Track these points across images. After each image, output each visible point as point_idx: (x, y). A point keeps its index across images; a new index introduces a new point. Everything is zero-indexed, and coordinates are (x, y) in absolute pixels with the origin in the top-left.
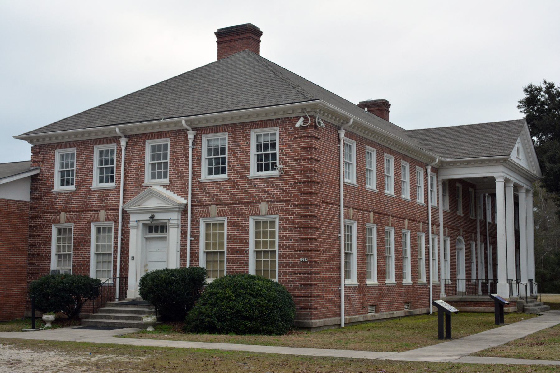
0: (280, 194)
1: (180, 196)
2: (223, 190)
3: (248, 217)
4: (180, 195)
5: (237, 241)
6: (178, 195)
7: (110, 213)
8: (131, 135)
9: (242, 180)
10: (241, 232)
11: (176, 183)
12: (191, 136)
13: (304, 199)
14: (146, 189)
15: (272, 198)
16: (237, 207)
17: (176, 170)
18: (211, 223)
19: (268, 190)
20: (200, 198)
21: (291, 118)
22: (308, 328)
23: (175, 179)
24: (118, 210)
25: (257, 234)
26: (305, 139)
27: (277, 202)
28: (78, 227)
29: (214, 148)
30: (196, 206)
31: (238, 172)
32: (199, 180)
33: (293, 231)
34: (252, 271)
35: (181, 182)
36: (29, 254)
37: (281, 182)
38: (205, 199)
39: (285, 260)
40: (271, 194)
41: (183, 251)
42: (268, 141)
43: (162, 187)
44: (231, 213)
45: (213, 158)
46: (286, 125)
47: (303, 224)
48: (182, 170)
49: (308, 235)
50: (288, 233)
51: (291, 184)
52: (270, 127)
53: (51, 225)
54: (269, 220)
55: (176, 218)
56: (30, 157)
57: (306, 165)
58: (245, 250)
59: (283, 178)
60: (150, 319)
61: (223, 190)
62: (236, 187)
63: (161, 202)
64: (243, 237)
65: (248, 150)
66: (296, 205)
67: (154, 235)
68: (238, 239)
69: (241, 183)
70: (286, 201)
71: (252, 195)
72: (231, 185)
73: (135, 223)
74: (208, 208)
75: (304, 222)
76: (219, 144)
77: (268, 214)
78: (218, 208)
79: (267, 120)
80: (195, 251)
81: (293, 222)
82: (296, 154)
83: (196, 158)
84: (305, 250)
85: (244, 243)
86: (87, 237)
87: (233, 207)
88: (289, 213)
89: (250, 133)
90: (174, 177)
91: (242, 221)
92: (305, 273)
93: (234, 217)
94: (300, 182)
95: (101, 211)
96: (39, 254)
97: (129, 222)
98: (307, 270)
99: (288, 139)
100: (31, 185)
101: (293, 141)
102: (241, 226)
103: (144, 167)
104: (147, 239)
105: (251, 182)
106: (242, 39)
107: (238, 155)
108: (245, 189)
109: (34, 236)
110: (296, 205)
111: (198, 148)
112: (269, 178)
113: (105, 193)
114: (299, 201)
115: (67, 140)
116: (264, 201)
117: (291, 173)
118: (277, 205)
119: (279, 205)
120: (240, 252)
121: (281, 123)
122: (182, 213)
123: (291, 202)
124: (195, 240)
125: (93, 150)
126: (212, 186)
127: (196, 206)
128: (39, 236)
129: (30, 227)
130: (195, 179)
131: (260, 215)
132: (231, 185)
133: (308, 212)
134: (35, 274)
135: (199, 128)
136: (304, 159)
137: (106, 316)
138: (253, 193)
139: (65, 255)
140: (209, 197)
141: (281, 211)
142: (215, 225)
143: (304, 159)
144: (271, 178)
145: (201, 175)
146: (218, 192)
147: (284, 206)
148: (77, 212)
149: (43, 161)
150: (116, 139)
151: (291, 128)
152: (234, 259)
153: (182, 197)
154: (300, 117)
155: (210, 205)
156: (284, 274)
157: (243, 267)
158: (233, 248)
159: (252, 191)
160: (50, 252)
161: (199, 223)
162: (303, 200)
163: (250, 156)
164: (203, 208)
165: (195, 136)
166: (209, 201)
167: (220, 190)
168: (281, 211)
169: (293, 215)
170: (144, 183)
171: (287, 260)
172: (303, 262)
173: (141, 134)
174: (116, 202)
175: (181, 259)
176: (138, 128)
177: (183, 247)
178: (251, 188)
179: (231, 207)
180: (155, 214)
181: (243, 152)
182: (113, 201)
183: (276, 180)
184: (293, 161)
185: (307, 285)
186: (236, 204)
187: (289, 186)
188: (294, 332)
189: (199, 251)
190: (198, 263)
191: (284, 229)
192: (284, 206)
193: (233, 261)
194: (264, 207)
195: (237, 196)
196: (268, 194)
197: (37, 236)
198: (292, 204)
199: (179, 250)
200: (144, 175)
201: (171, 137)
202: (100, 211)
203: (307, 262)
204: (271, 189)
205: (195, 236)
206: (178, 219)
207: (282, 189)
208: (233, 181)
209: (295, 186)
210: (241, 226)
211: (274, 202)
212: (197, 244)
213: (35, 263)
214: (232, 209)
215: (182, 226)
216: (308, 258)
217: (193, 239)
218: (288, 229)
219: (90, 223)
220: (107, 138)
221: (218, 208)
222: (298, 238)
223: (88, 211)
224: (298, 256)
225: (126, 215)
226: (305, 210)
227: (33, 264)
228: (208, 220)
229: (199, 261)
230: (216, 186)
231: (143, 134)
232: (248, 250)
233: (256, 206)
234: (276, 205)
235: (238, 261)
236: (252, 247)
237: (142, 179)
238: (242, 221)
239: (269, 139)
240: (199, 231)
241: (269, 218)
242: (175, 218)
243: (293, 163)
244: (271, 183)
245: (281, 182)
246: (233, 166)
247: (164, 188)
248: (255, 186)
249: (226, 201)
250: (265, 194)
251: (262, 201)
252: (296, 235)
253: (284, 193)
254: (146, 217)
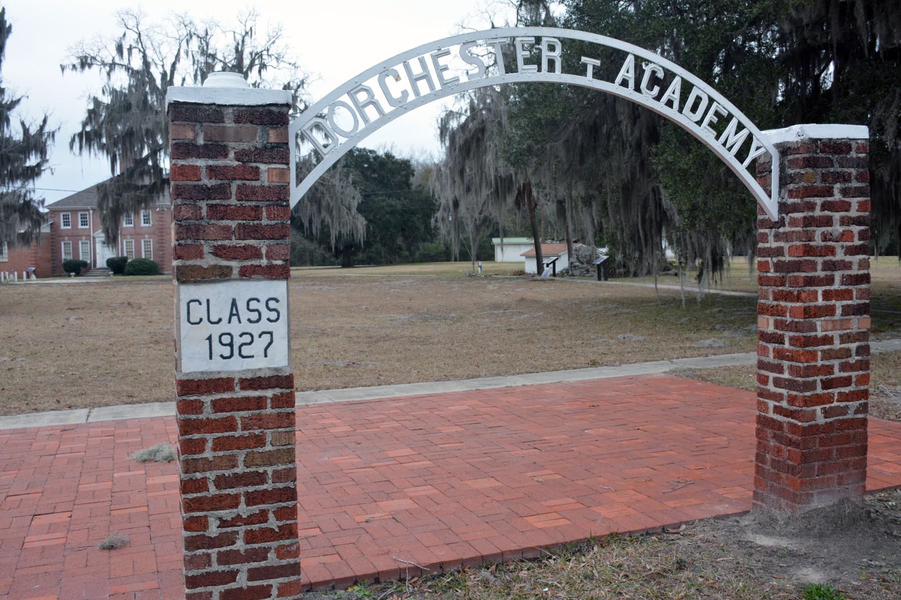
34: (143, 257)
38: (126, 233)
57: (160, 223)
60: (112, 273)
150: (88, 210)
162: (160, 234)
194: (147, 236)
225: (94, 238)
252: (158, 245)
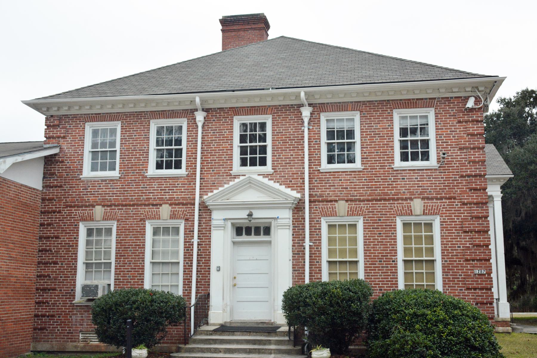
0: (440, 189)
1: (290, 189)
2: (356, 182)
3: (395, 217)
4: (289, 187)
5: (380, 248)
6: (286, 187)
7: (179, 209)
8: (211, 109)
9: (384, 171)
10: (385, 236)
11: (283, 171)
12: (306, 112)
13: (476, 196)
14: (235, 178)
15: (430, 194)
16: (378, 204)
17: (283, 156)
18: (337, 223)
19: (422, 184)
20: (321, 191)
21: (452, 98)
23: (281, 166)
24: (194, 204)
25: (407, 239)
26: (472, 123)
27: (437, 199)
28: (123, 227)
29: (347, 131)
30: (315, 201)
31: (377, 161)
32: (319, 168)
33: (461, 236)
34: (401, 286)
35: (291, 171)
36: (39, 263)
37: (441, 175)
38: (329, 193)
39: (452, 272)
40: (428, 189)
41: (296, 259)
42: (417, 125)
43: (261, 177)
44: (368, 212)
45: (335, 143)
46: (445, 106)
47: (477, 227)
48: (292, 155)
49: (485, 241)
50: (454, 239)
51: (455, 178)
52: (421, 107)
53: (79, 223)
54: (423, 222)
55: (288, 216)
56: (44, 130)
58: (392, 259)
59: (443, 170)
61: (356, 182)
62: (374, 179)
63: (262, 195)
64: (389, 242)
65: (391, 134)
66: (464, 204)
67: (244, 238)
68: (381, 245)
69: (382, 174)
70: (450, 198)
71: (400, 190)
72: (367, 177)
73: (222, 222)
74: (335, 205)
75: (478, 224)
76: (346, 126)
77: (424, 214)
78: (349, 205)
79: (417, 99)
80: (316, 259)
81: (461, 225)
82: (461, 141)
83: (313, 142)
84: (480, 260)
85: (390, 250)
86: (140, 240)
87: (372, 204)
88: (455, 213)
89: (392, 113)
90: (280, 164)
91: (387, 223)
92: (482, 289)
93: (374, 217)
94: (469, 176)
95: (163, 205)
96: (56, 263)
97: (210, 220)
98: (486, 284)
99: (449, 123)
100: (44, 168)
101: (456, 126)
102: (384, 228)
103: (232, 150)
104: (234, 243)
105: (396, 174)
106: (255, 29)
107: (377, 139)
108: (389, 182)
109: (48, 238)
110: (464, 204)
111: (316, 129)
112: (423, 170)
113: (169, 182)
114: (469, 199)
115: (107, 110)
116: (419, 198)
117: (454, 164)
118: (437, 203)
119: (440, 203)
120: (384, 261)
121: (437, 104)
122: (293, 210)
123: (457, 199)
124: (315, 246)
125: (149, 125)
126: (339, 178)
127: (315, 201)
128: (57, 237)
129: (42, 225)
130: (313, 168)
131: (412, 215)
132: (367, 177)
133: (483, 213)
134: (49, 290)
135: (316, 104)
136: (474, 148)
137: (210, 348)
138: (400, 187)
139: (99, 265)
140: (335, 191)
141: (442, 211)
142: (342, 226)
143: (474, 148)
144: (426, 170)
145: (320, 162)
146: (349, 185)
147: (447, 205)
148: (123, 205)
151: (453, 110)
152: (375, 270)
153: (292, 190)
154: (469, 97)
155: (336, 201)
156: (451, 290)
157: (389, 281)
158: (374, 256)
159: (399, 184)
160: (76, 260)
161: (320, 224)
163: (393, 141)
164: (326, 205)
165: (311, 114)
166: (336, 196)
167: (350, 183)
168: (442, 211)
169: (461, 216)
170: (232, 170)
171: (456, 272)
172: (478, 274)
173: (227, 108)
174: (188, 195)
175: (294, 271)
176: (226, 99)
177: (296, 254)
178: (397, 182)
179: (369, 204)
180: (253, 211)
181: (384, 136)
182: (182, 192)
183: (434, 173)
184: (457, 150)
185: (487, 303)
186: (377, 200)
187: (452, 180)
189: (321, 260)
190: (321, 276)
191: (448, 233)
192: (447, 205)
193: (374, 273)
194: (417, 205)
195: (377, 190)
196: (422, 189)
197: (52, 238)
198: (458, 202)
199: (291, 258)
200: (232, 160)
201: (274, 113)
202: (161, 205)
203: (484, 275)
204: (428, 184)
205: (315, 240)
206: (289, 219)
207: (442, 183)
208: (370, 172)
209: (461, 180)
210: (384, 228)
211: (432, 199)
212: (318, 251)
213: (49, 276)
214: (370, 207)
215: (293, 227)
216: (487, 270)
217: (311, 244)
218: (454, 233)
219: (145, 221)
220: (172, 110)
221: (349, 205)
222: (469, 244)
223: (141, 205)
224: (470, 267)
226: (479, 210)
227: (45, 276)
228: (333, 220)
229: (321, 273)
230: (345, 177)
231: (230, 108)
232: (397, 259)
233: (406, 203)
234: (435, 203)
235: (382, 273)
236: (400, 256)
237: (229, 165)
238: (387, 223)
239: (419, 122)
240: (321, 234)
241: (427, 219)
242: (286, 215)
243: (458, 153)
244: (427, 176)
245: (441, 175)
246: (369, 153)
247: (263, 177)
248: (404, 179)
249: (362, 196)
250: (419, 189)
251: (415, 198)
252: (466, 241)
253: (446, 189)
254: (243, 214)
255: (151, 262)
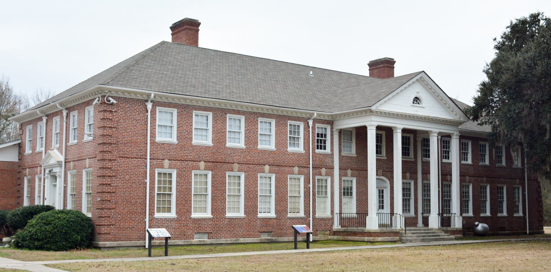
22: (98, 248)
106: (183, 30)
149: (22, 134)
188: (86, 249)
217: (65, 185)
255: (86, 193)
